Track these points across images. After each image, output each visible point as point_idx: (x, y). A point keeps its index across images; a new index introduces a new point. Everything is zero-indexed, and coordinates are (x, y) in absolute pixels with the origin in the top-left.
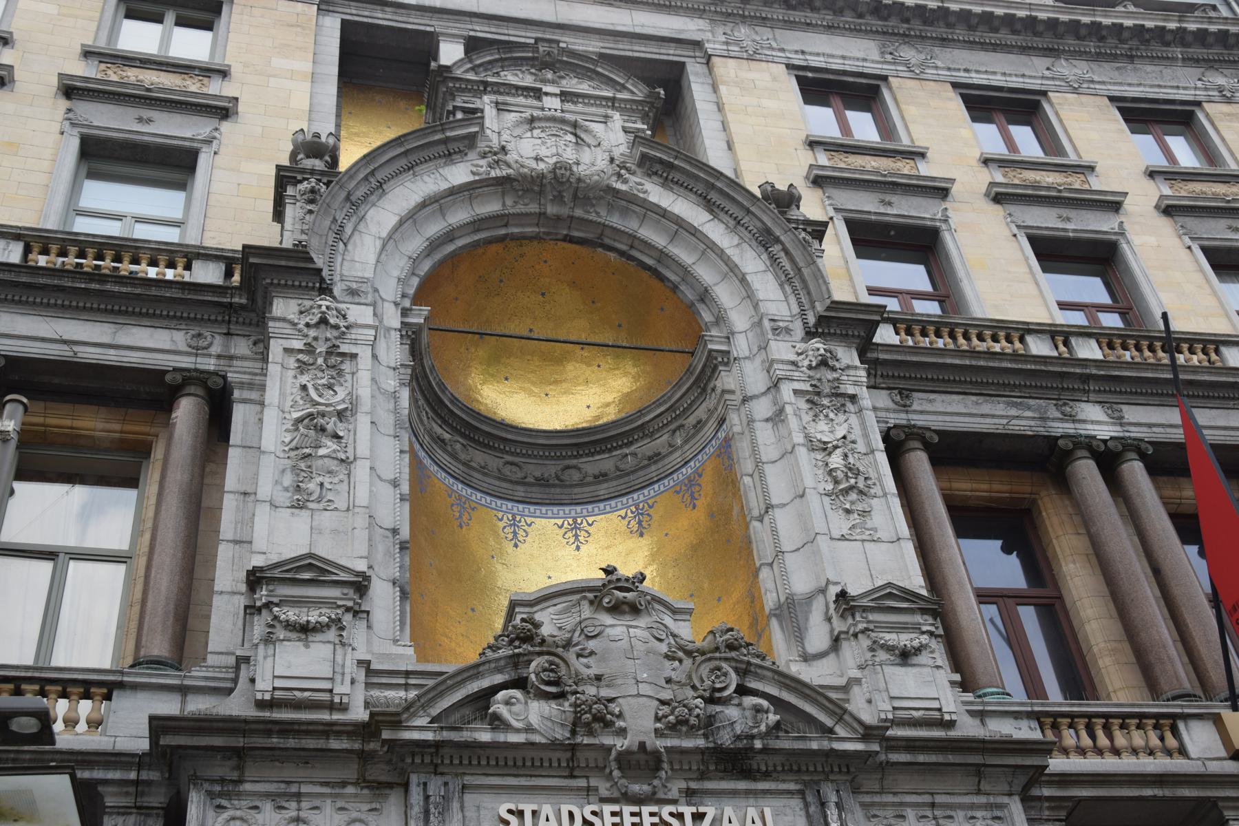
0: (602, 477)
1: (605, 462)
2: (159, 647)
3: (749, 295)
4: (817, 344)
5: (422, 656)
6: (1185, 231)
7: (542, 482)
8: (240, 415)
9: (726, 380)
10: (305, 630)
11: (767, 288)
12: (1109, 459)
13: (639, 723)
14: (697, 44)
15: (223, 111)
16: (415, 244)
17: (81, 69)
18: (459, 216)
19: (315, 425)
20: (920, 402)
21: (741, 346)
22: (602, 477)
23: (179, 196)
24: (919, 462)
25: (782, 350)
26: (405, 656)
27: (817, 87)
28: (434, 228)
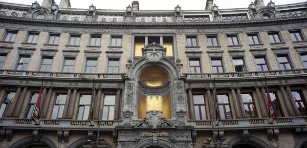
0: (160, 92)
1: (160, 90)
2: (117, 118)
3: (173, 75)
4: (179, 81)
5: (139, 118)
6: (230, 55)
7: (154, 93)
8: (123, 93)
9: (170, 84)
10: (127, 117)
11: (175, 74)
12: (211, 90)
13: (155, 127)
14: (175, 33)
15: (122, 53)
16: (139, 71)
17: (107, 50)
18: (143, 67)
19: (129, 95)
20: (191, 85)
21: (172, 81)
22: (160, 92)
23: (118, 62)
24: (190, 92)
25: (175, 82)
26: (137, 118)
27: (188, 37)
28: (141, 69)
